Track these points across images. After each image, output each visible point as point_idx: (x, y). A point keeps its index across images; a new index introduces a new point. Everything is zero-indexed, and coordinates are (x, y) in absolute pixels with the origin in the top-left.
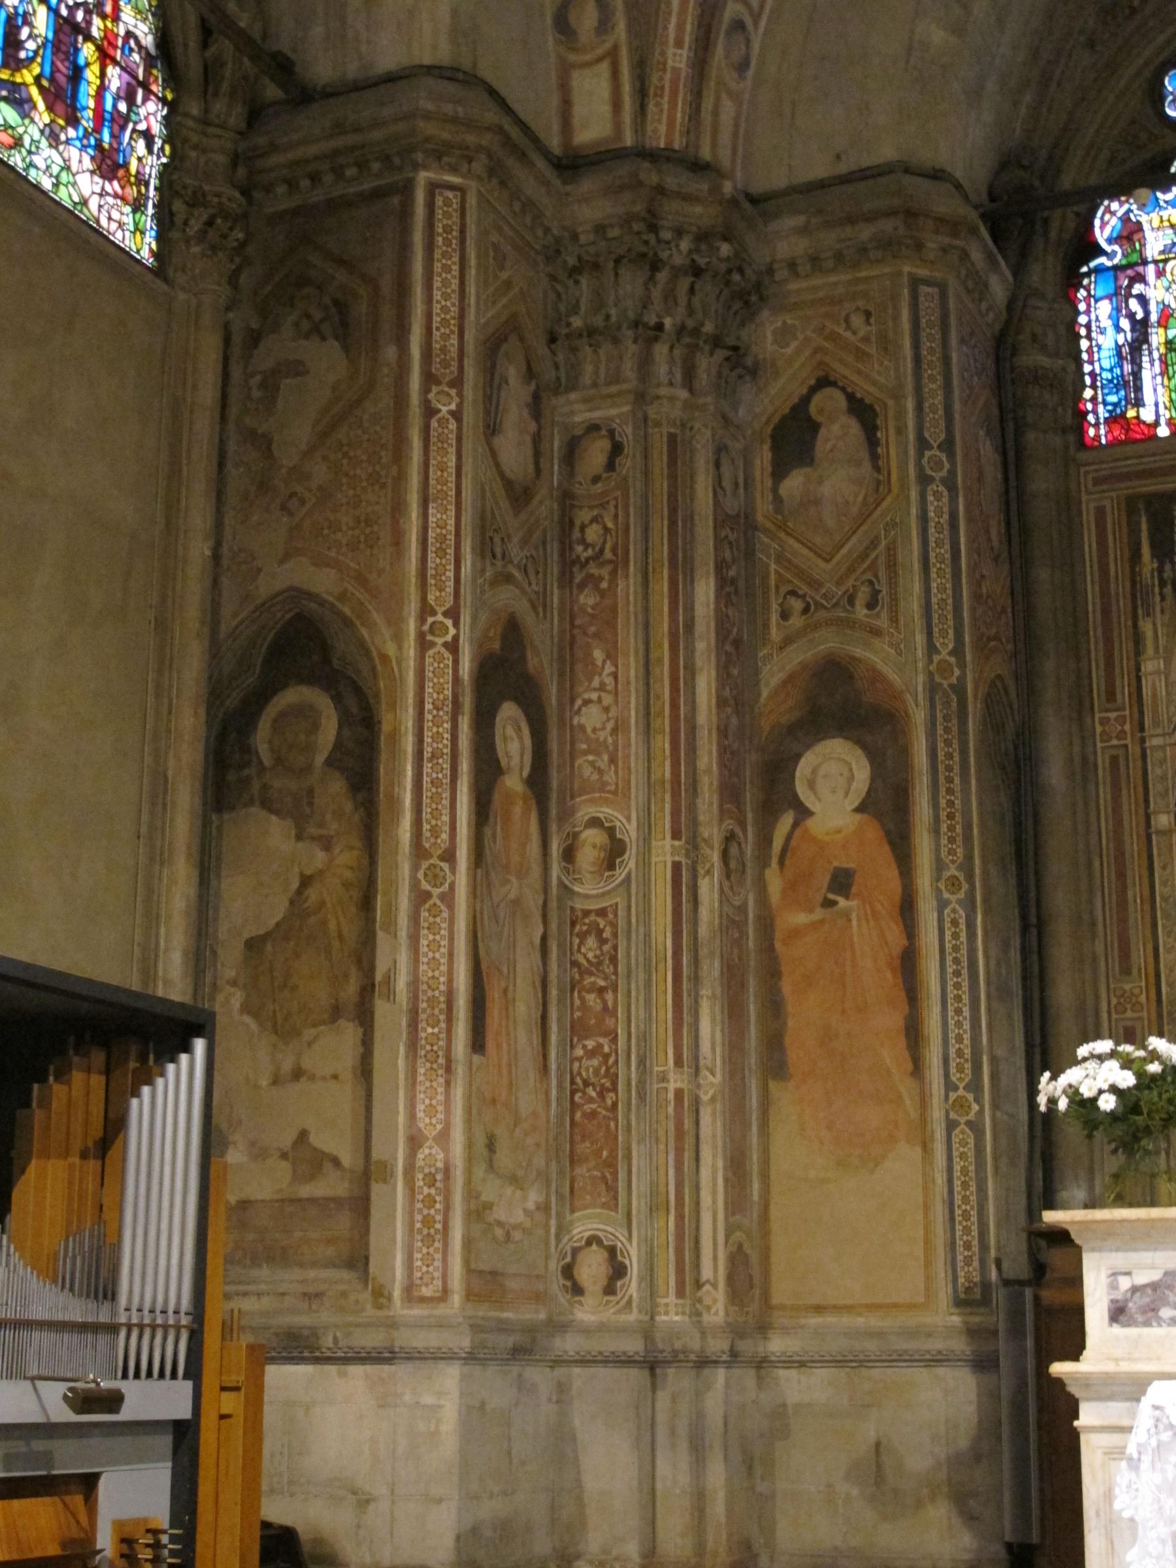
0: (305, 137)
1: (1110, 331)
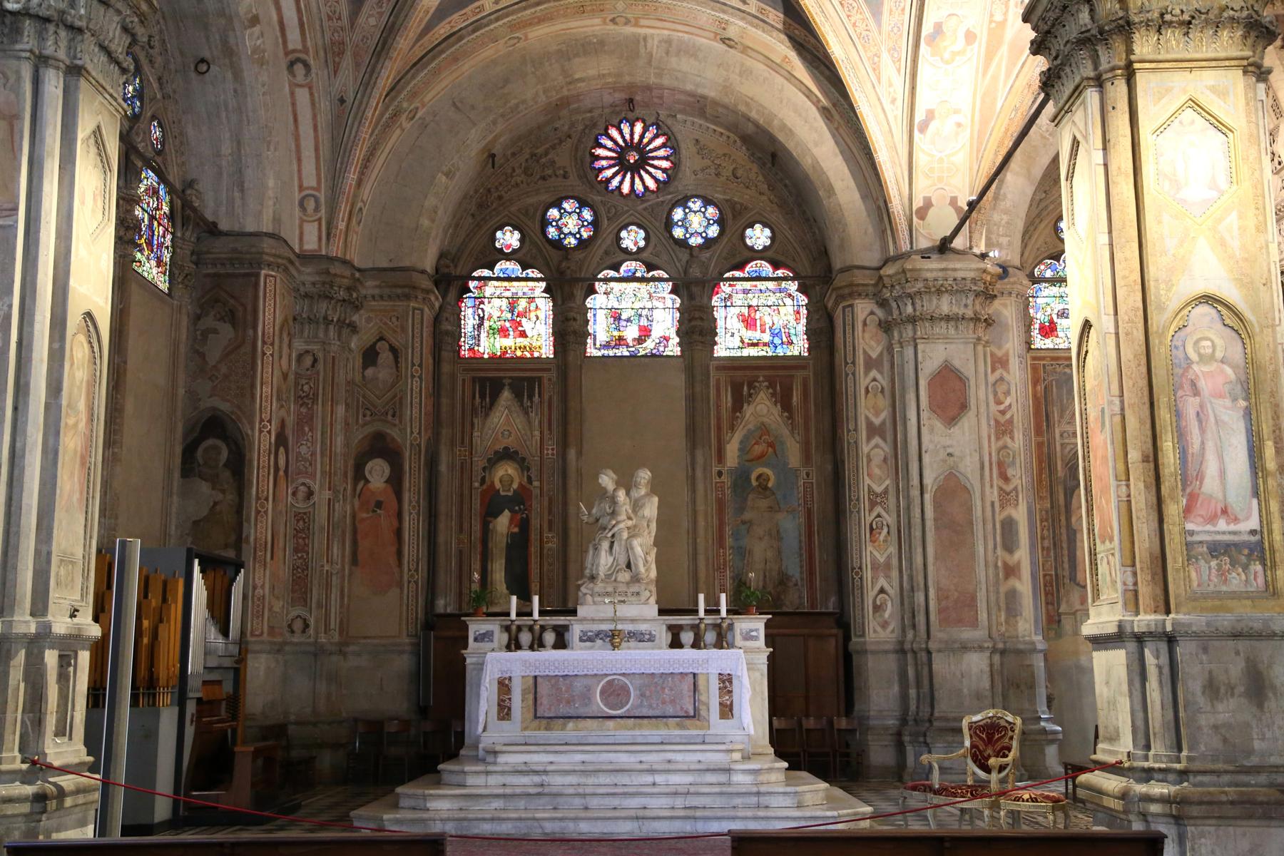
0: (220, 247)
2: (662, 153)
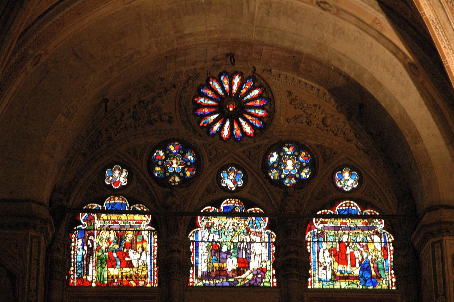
1: (81, 249)
2: (258, 103)
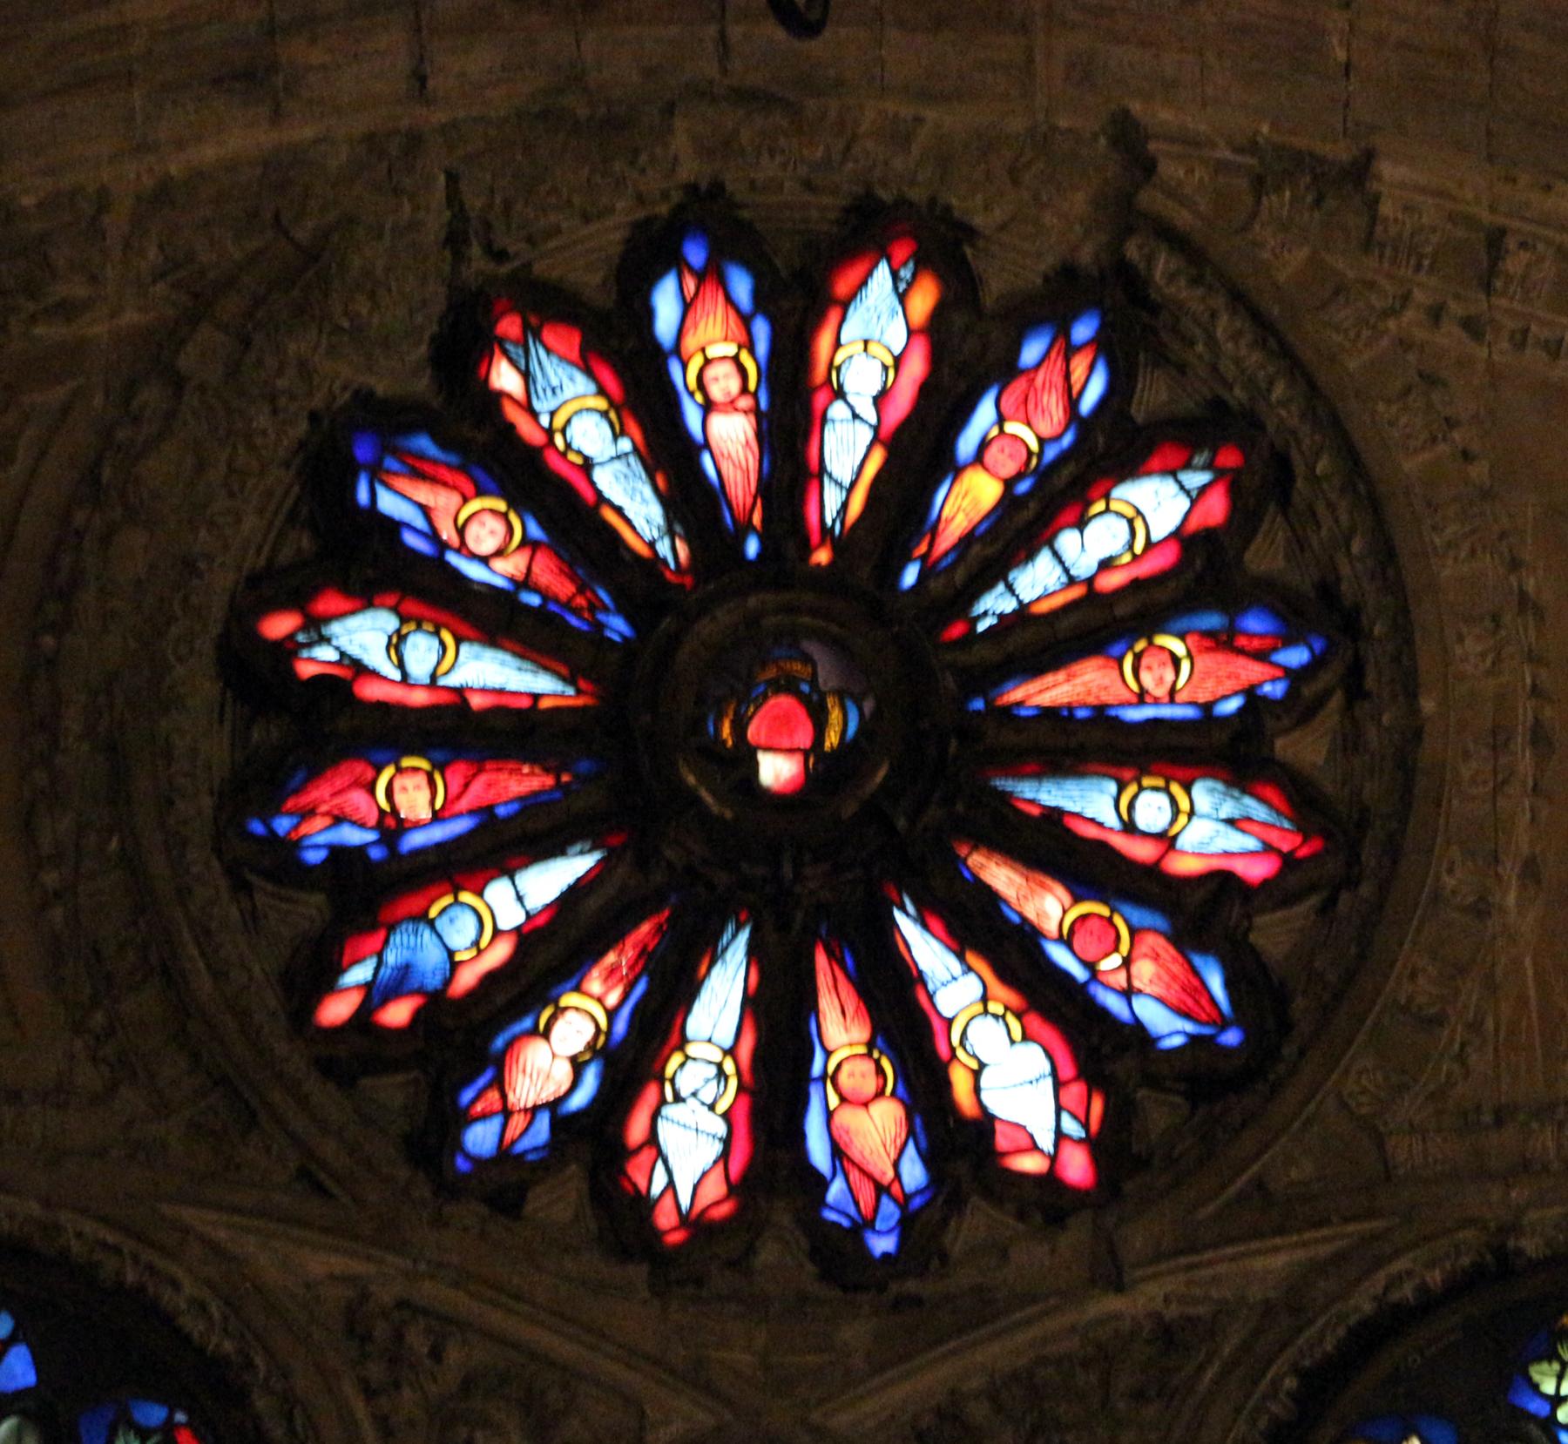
2: (1172, 676)
